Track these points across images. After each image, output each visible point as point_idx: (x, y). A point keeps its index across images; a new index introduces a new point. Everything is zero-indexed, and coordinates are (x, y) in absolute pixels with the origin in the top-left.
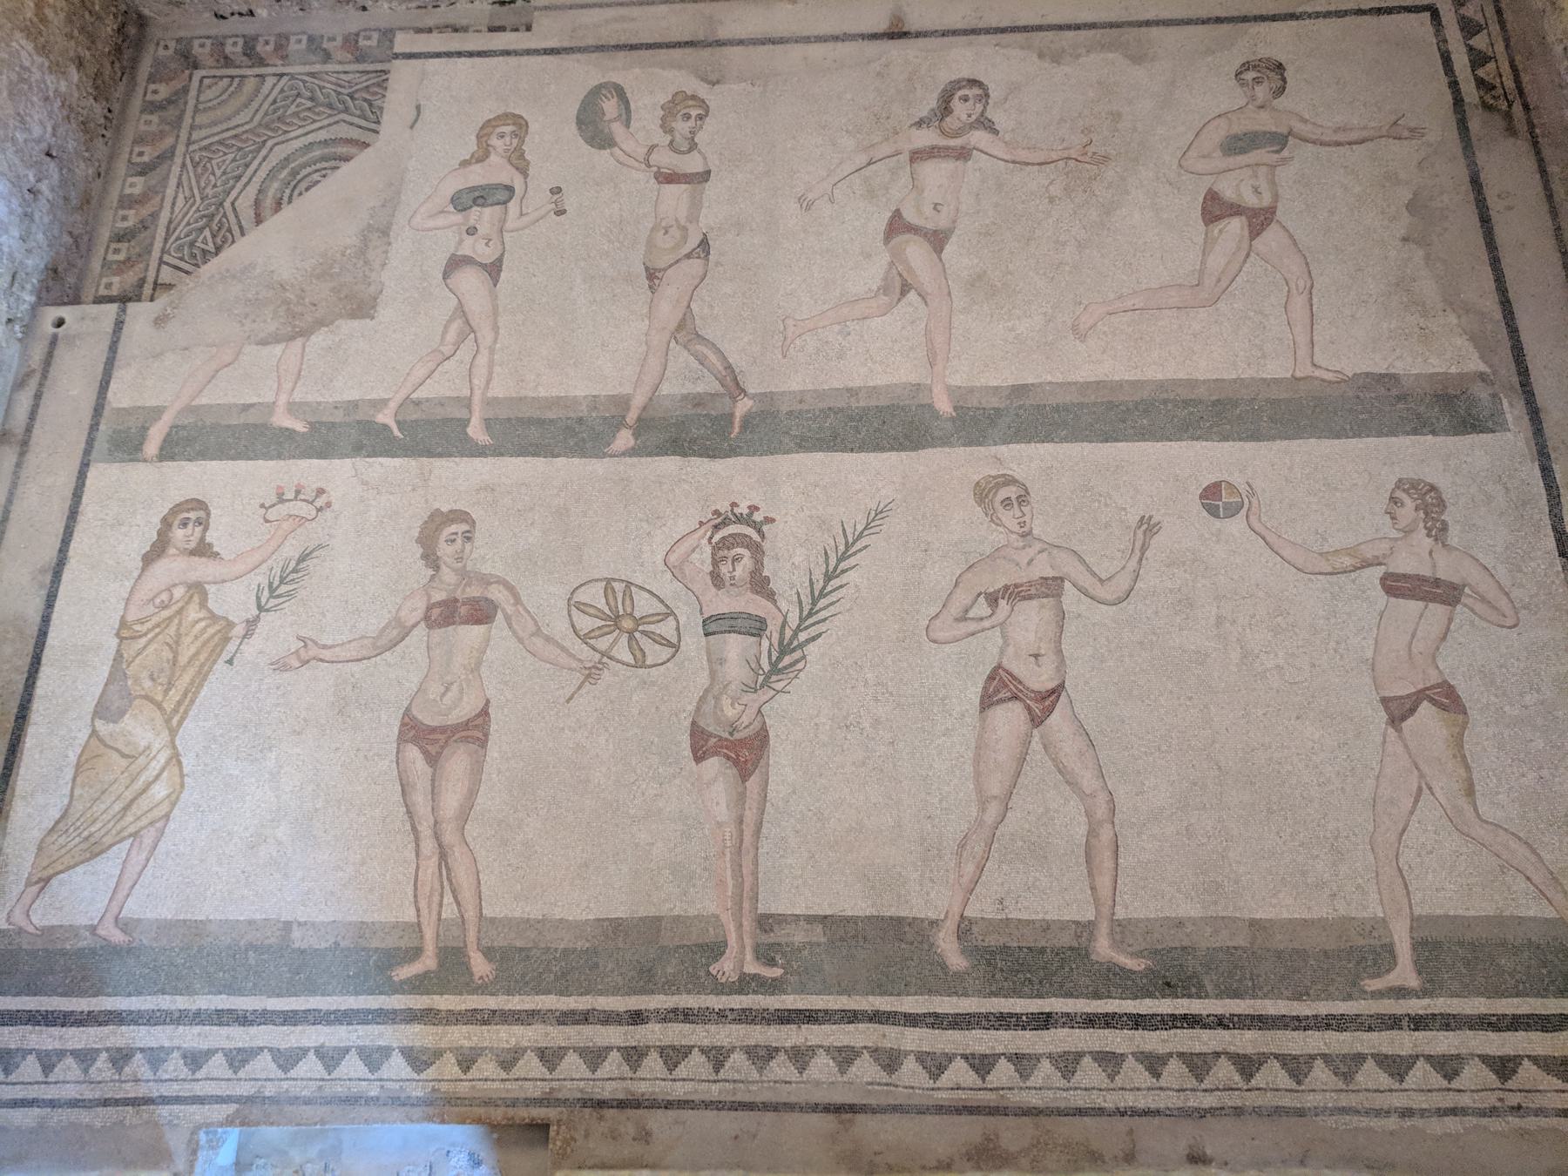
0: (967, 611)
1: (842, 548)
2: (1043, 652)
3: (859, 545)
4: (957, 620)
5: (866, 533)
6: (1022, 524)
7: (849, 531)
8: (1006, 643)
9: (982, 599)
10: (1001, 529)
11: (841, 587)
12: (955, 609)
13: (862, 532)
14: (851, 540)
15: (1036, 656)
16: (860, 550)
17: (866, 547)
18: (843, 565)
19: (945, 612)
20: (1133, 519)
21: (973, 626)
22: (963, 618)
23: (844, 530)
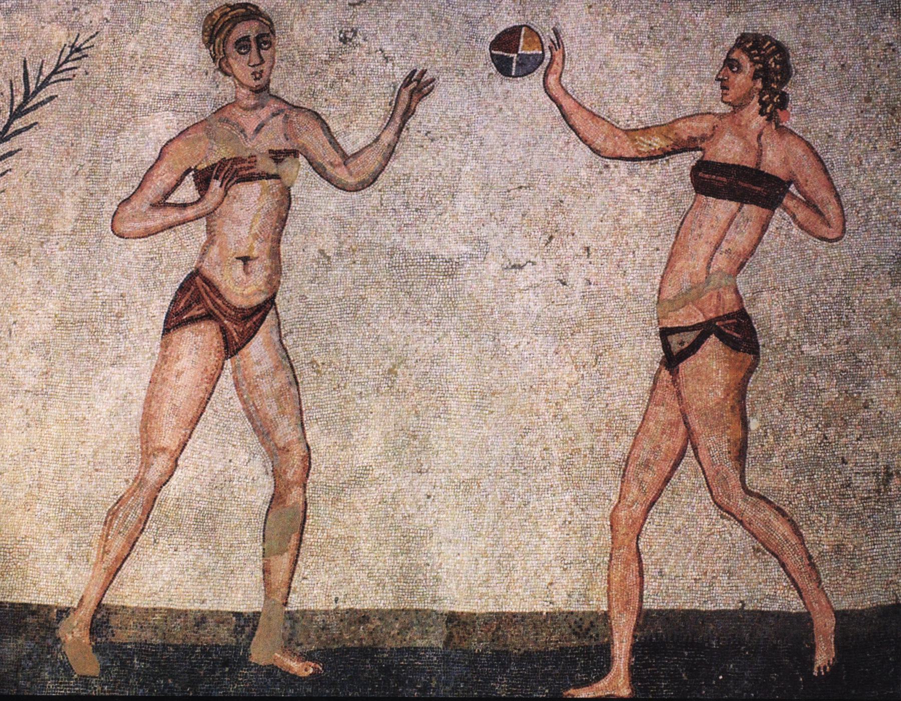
0: (167, 195)
1: (19, 99)
2: (255, 253)
3: (43, 95)
4: (155, 206)
5: (54, 78)
6: (257, 75)
7: (32, 74)
8: (211, 242)
9: (189, 179)
10: (229, 80)
11: (11, 154)
12: (152, 192)
13: (49, 77)
14: (32, 87)
15: (245, 260)
16: (43, 103)
17: (51, 98)
18: (18, 124)
19: (140, 195)
20: (400, 76)
21: (174, 216)
22: (161, 204)
23: (26, 74)
